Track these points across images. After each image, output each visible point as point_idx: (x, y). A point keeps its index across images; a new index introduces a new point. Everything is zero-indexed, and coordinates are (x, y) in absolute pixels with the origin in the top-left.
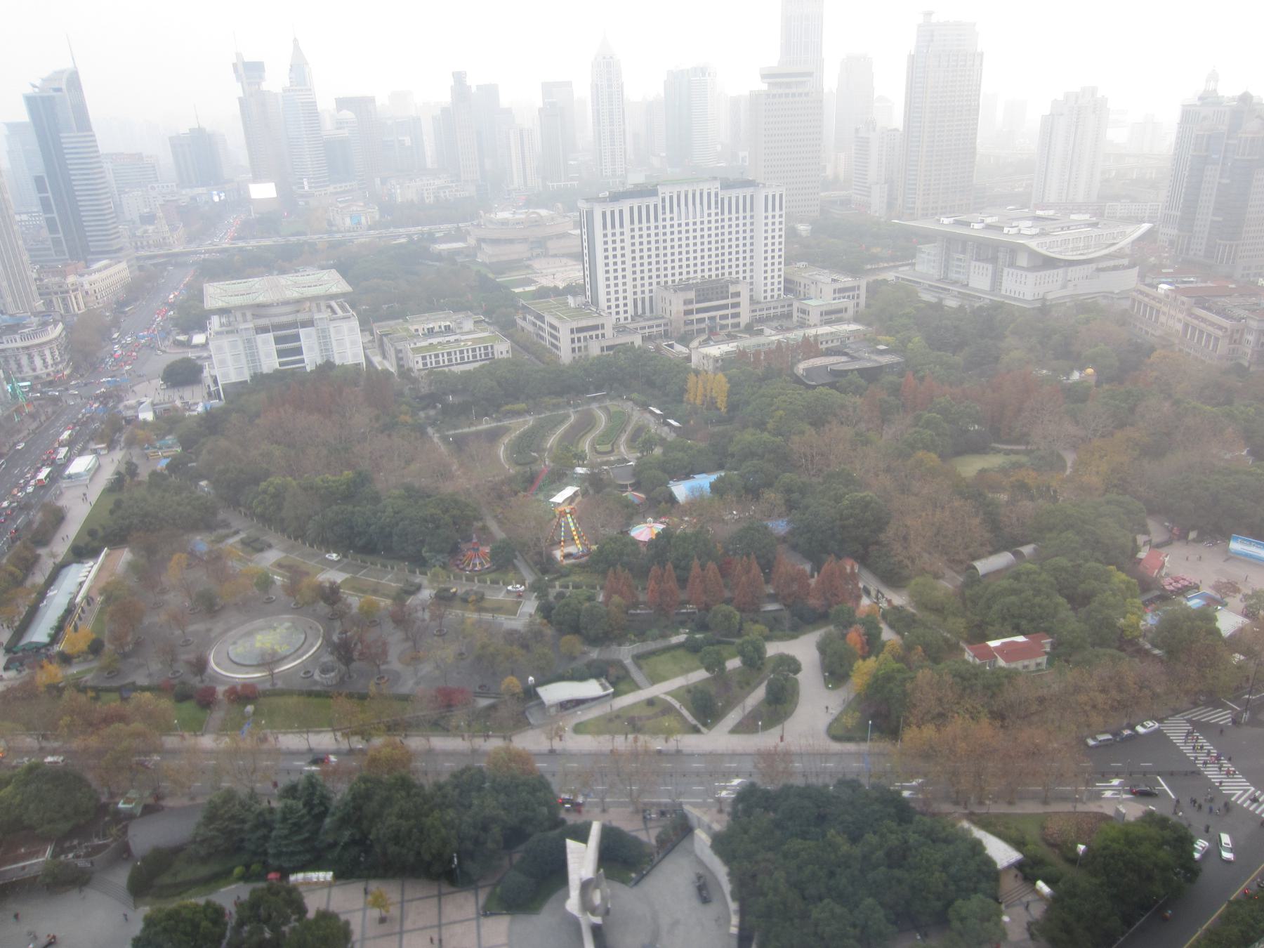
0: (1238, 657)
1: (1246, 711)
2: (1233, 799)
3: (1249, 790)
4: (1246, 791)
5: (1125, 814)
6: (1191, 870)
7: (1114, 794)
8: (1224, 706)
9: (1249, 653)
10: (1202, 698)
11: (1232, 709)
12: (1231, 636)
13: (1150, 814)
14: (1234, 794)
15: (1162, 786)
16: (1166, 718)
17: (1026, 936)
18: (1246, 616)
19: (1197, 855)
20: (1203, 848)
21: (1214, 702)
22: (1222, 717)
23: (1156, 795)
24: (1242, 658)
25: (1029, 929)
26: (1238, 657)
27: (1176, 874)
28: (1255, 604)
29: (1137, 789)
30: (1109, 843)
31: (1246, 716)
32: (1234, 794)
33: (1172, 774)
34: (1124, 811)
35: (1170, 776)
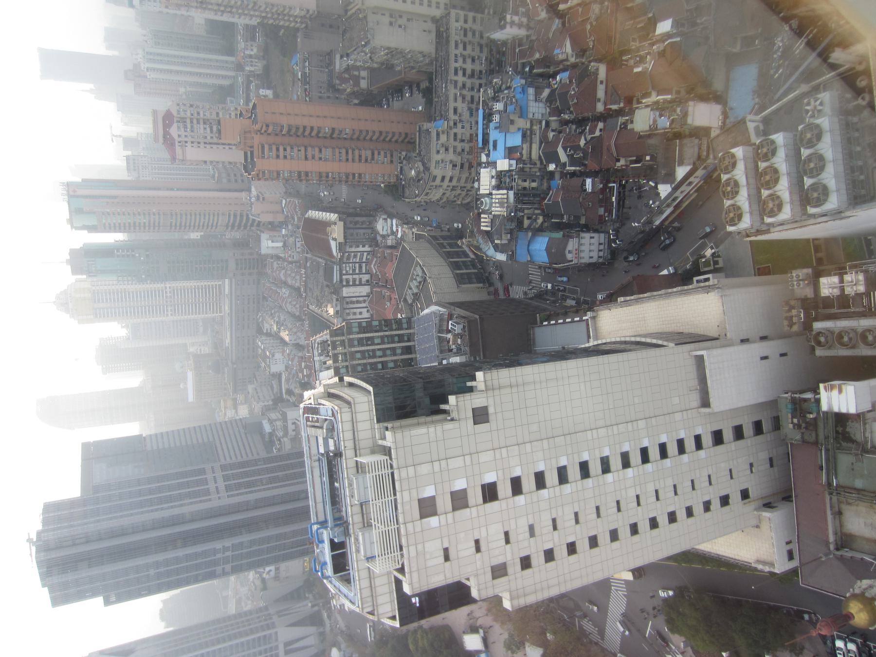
0: (549, 636)
1: (575, 616)
2: (626, 593)
3: (615, 589)
4: (617, 590)
5: (683, 642)
6: (680, 592)
7: (677, 654)
8: (581, 627)
9: (543, 633)
10: (585, 641)
11: (579, 622)
12: (540, 647)
13: (671, 630)
14: (623, 594)
15: (650, 631)
16: (612, 653)
17: (805, 651)
18: (524, 644)
19: (671, 593)
20: (664, 592)
21: (583, 633)
22: (588, 626)
23: (657, 631)
24: (548, 635)
25: (801, 653)
26: (549, 636)
27: (690, 597)
28: (514, 645)
29: (663, 643)
30: (707, 642)
31: (578, 614)
32: (623, 594)
33: (639, 630)
34: (682, 644)
35: (642, 632)
